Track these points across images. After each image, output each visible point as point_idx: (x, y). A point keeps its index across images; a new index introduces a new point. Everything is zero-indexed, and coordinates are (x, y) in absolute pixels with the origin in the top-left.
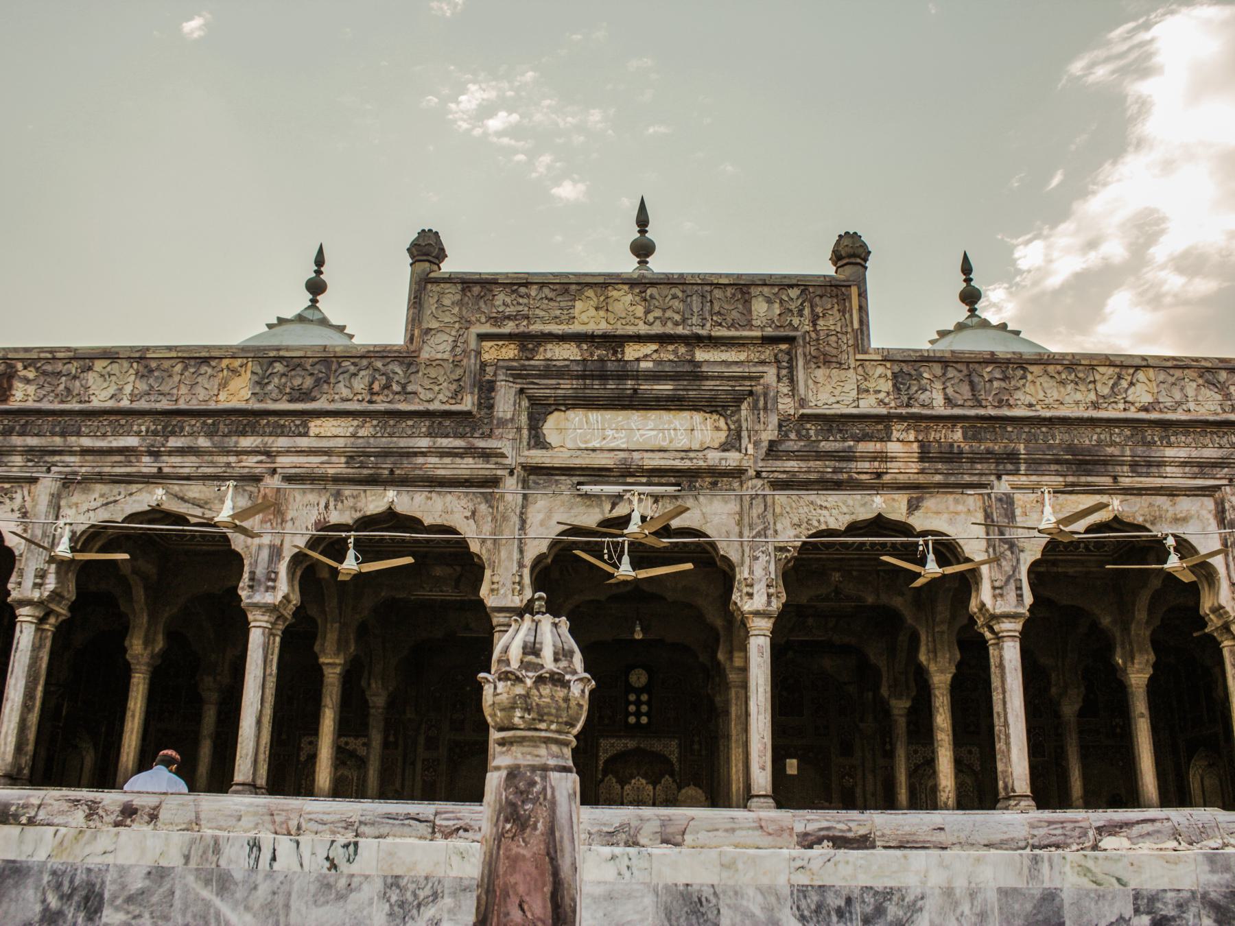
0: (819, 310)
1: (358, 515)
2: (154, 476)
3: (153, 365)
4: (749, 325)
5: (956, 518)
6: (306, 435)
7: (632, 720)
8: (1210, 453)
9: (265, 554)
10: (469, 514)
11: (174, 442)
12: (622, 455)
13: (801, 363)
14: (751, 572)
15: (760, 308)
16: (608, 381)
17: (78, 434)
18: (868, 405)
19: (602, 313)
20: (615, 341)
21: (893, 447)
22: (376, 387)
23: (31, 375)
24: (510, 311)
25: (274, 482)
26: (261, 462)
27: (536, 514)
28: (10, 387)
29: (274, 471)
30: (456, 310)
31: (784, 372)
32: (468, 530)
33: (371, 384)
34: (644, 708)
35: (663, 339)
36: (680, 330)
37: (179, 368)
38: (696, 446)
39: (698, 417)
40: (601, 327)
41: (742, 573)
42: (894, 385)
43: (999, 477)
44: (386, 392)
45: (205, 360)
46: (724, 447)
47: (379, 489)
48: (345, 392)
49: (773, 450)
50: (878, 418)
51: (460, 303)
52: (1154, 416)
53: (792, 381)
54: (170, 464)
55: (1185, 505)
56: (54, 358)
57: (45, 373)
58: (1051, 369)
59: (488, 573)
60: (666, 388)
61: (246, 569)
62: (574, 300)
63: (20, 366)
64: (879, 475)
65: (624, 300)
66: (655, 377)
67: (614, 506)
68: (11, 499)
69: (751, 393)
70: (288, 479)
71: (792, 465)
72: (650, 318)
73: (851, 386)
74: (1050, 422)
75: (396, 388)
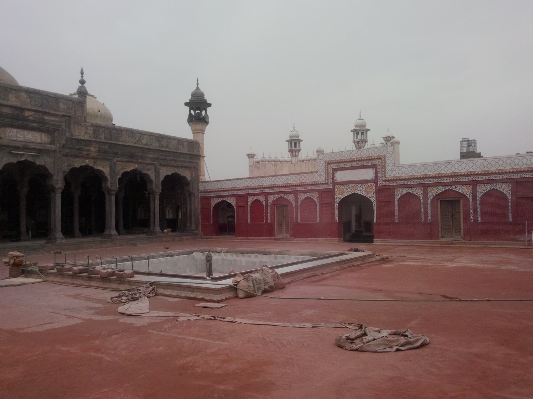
0: (76, 109)
5: (104, 168)
8: (156, 156)
12: (23, 143)
15: (62, 106)
18: (87, 137)
20: (22, 110)
21: (92, 149)
35: (36, 111)
36: (41, 110)
38: (43, 142)
39: (43, 134)
40: (18, 104)
41: (55, 178)
49: (64, 147)
50: (90, 141)
52: (146, 147)
55: (149, 167)
60: (35, 125)
64: (88, 155)
66: (33, 121)
67: (21, 157)
69: (58, 130)
71: (68, 150)
72: (32, 103)
73: (83, 131)
74: (126, 146)
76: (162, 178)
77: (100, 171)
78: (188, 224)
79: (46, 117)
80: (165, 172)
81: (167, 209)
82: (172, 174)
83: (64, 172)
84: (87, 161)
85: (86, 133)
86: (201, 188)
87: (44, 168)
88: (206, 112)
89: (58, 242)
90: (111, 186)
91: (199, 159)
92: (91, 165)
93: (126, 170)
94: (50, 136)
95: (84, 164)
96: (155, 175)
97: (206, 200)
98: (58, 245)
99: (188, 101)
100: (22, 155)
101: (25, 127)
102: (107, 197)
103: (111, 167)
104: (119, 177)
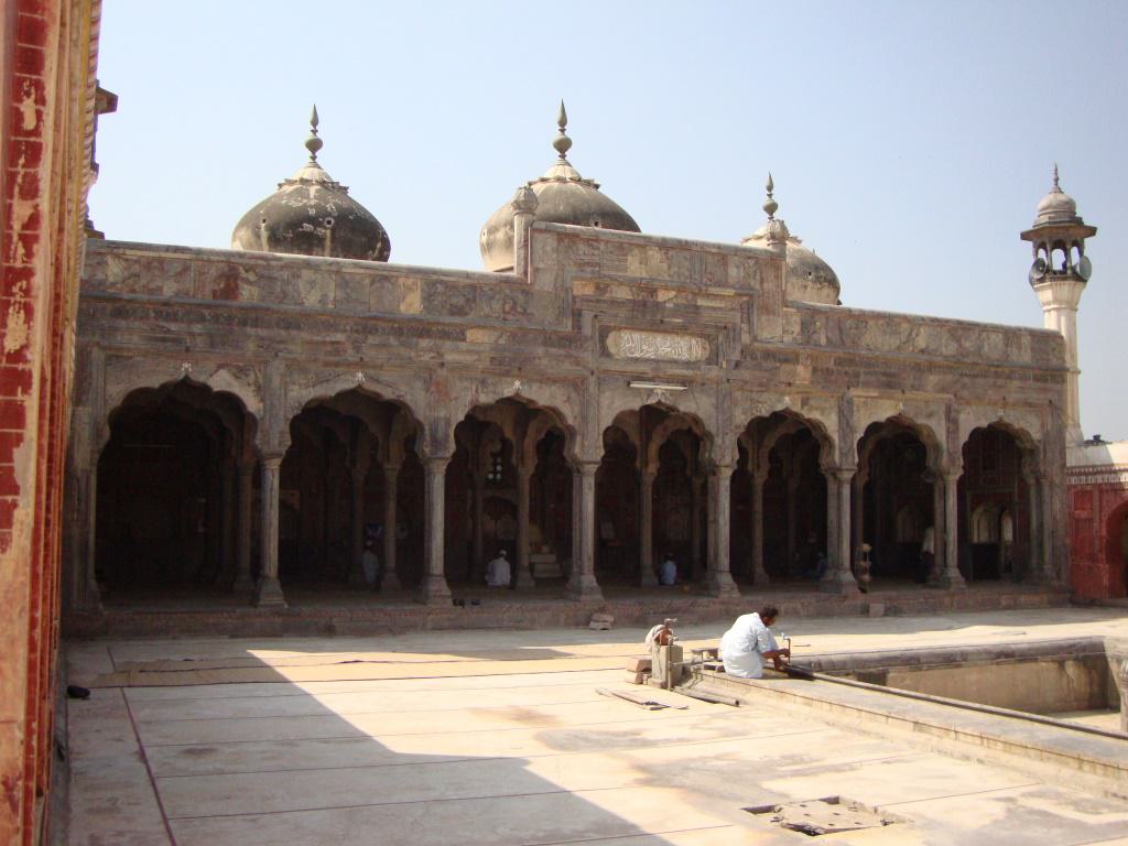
1: (497, 397)
2: (356, 364)
3: (347, 277)
4: (724, 285)
6: (464, 340)
7: (499, 476)
9: (442, 423)
10: (565, 399)
11: (372, 340)
13: (755, 313)
14: (723, 442)
15: (733, 272)
16: (646, 313)
17: (298, 328)
19: (643, 266)
21: (800, 369)
22: (507, 308)
23: (252, 277)
24: (586, 259)
25: (443, 372)
26: (433, 358)
27: (605, 402)
28: (237, 286)
29: (442, 365)
30: (555, 256)
31: (745, 315)
32: (566, 410)
33: (504, 305)
34: (499, 468)
37: (367, 281)
38: (693, 359)
39: (694, 341)
41: (718, 441)
42: (802, 330)
43: (849, 388)
44: (513, 312)
45: (386, 278)
46: (709, 361)
47: (509, 379)
48: (487, 310)
51: (557, 251)
53: (749, 322)
54: (369, 354)
56: (269, 265)
57: (262, 276)
58: (881, 322)
59: (578, 439)
61: (427, 432)
62: (626, 255)
63: (241, 268)
65: (656, 256)
67: (649, 396)
68: (247, 376)
69: (725, 328)
70: (452, 370)
72: (672, 272)
73: (779, 331)
75: (519, 310)
76: (964, 437)
77: (817, 426)
78: (1034, 561)
79: (700, 302)
80: (972, 420)
81: (975, 517)
82: (990, 426)
83: (737, 427)
84: (787, 398)
85: (784, 331)
86: (1073, 458)
87: (696, 420)
88: (1081, 253)
89: (724, 596)
90: (841, 458)
91: (1064, 381)
92: (796, 408)
93: (875, 419)
94: (707, 346)
95: (779, 407)
96: (948, 431)
97: (1082, 496)
98: (722, 603)
99: (1029, 227)
100: (650, 392)
101: (659, 327)
102: (832, 487)
103: (841, 413)
104: (860, 434)
